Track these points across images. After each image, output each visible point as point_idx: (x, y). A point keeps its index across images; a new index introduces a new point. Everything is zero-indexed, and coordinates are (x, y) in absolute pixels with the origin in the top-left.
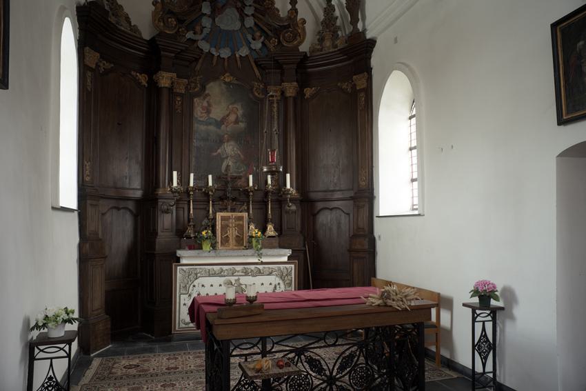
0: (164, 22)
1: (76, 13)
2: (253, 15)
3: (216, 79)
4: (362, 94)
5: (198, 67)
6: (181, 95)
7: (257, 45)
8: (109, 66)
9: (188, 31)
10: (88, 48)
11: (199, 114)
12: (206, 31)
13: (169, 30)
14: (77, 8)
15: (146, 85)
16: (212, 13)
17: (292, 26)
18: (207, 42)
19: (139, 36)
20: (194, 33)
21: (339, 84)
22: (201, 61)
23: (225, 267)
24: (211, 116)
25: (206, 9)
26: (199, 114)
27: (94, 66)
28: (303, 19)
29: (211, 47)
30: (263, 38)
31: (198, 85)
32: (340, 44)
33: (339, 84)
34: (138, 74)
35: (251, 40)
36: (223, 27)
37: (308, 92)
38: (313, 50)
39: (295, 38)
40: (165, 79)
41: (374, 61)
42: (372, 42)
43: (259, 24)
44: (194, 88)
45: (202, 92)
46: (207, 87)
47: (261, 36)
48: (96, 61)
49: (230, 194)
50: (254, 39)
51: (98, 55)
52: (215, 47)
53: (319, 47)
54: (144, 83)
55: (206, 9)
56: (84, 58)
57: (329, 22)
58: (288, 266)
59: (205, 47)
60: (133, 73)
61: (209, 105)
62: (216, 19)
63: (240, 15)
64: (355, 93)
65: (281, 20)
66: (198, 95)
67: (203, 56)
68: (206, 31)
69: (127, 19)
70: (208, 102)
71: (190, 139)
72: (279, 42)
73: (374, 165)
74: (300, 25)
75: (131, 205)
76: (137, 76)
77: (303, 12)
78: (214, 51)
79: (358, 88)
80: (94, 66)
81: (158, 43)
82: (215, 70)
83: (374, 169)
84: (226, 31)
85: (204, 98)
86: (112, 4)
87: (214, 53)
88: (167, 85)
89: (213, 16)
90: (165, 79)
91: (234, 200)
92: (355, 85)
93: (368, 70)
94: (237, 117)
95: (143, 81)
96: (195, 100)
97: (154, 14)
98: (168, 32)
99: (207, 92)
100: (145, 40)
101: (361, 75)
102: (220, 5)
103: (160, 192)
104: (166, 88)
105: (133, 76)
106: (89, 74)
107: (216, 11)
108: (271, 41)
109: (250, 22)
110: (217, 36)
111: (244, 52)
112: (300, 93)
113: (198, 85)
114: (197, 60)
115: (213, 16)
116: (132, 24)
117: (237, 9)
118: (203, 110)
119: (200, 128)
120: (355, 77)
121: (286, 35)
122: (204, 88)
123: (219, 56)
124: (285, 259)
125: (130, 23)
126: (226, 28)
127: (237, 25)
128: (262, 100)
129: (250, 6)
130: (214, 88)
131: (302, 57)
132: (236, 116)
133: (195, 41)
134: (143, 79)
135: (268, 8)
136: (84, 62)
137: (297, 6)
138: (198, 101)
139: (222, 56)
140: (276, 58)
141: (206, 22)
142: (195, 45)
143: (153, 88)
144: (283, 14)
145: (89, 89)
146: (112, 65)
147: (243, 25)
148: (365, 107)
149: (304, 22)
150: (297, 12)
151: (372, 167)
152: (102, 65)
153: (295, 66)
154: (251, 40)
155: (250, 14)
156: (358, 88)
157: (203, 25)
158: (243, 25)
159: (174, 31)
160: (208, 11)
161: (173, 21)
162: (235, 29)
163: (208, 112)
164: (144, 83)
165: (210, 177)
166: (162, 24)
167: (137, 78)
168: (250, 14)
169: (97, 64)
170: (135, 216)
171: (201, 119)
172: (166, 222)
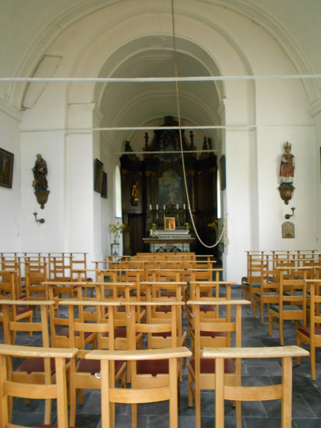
23: (167, 236)
37: (199, 173)
40: (148, 173)
45: (161, 176)
49: (171, 212)
58: (188, 235)
78: (165, 161)
90: (148, 173)
91: (173, 213)
103: (148, 211)
119: (161, 189)
124: (187, 233)
130: (166, 174)
134: (141, 174)
139: (168, 162)
143: (144, 175)
163: (163, 182)
164: (141, 175)
165: (164, 205)
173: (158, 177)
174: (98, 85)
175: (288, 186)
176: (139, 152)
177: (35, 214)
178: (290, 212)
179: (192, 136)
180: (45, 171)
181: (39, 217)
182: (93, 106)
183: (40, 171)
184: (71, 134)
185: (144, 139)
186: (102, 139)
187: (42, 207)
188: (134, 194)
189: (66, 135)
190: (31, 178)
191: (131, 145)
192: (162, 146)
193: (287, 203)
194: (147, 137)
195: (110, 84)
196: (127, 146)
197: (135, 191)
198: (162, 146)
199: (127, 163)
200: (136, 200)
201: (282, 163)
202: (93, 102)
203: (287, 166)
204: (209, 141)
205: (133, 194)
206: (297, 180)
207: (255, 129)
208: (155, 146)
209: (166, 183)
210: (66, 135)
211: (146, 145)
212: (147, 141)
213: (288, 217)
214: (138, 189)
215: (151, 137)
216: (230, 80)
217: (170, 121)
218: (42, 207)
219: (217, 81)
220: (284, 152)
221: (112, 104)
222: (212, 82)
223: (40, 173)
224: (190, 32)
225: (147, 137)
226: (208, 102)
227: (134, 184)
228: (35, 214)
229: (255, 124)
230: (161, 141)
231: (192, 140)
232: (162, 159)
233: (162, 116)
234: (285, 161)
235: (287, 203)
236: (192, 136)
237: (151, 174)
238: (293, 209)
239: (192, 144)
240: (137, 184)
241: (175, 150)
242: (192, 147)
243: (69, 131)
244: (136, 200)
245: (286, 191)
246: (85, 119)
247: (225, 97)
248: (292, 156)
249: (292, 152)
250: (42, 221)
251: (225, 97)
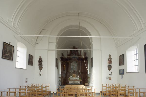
45: (72, 63)
49: (74, 72)
75: (65, 73)
90: (68, 62)
103: (68, 72)
119: (72, 66)
130: (73, 62)
134: (66, 62)
163: (72, 64)
170: (66, 74)
172: (68, 75)
174: (57, 37)
175: (110, 66)
176: (66, 56)
177: (39, 73)
178: (111, 73)
179: (80, 52)
180: (42, 61)
181: (40, 74)
182: (56, 43)
183: (40, 61)
184: (49, 51)
185: (67, 53)
186: (58, 53)
187: (41, 71)
189: (48, 51)
190: (38, 63)
191: (63, 54)
192: (72, 54)
193: (110, 71)
194: (68, 52)
195: (60, 37)
196: (63, 55)
198: (72, 54)
199: (62, 59)
200: (65, 69)
201: (109, 60)
202: (56, 42)
203: (110, 61)
204: (85, 53)
206: (112, 65)
207: (101, 51)
208: (70, 55)
209: (73, 65)
210: (48, 51)
211: (68, 54)
212: (68, 53)
213: (110, 75)
215: (69, 52)
216: (94, 37)
217: (74, 48)
218: (41, 71)
219: (90, 38)
220: (109, 57)
221: (61, 43)
222: (89, 38)
223: (40, 61)
224: (83, 25)
225: (68, 52)
226: (88, 43)
227: (64, 65)
228: (39, 73)
229: (101, 49)
230: (72, 53)
232: (72, 58)
233: (72, 46)
234: (109, 59)
235: (110, 71)
238: (112, 72)
239: (80, 54)
241: (76, 56)
242: (80, 55)
243: (49, 50)
244: (65, 69)
245: (110, 68)
246: (53, 47)
247: (93, 42)
248: (111, 58)
249: (111, 57)
250: (41, 75)
251: (93, 42)
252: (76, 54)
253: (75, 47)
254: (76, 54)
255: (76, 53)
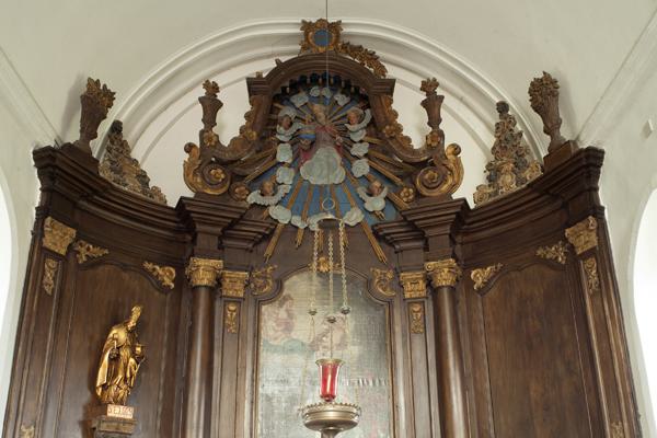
0: (203, 177)
1: (33, 163)
2: (366, 155)
3: (302, 267)
4: (592, 262)
5: (269, 251)
6: (238, 301)
7: (376, 204)
8: (97, 252)
9: (250, 192)
10: (49, 218)
11: (271, 333)
12: (282, 191)
13: (212, 189)
14: (35, 153)
15: (173, 285)
16: (294, 160)
17: (438, 160)
18: (286, 207)
19: (162, 203)
20: (262, 195)
21: (539, 252)
22: (274, 239)
24: (294, 335)
25: (284, 154)
26: (271, 333)
27: (63, 252)
28: (453, 145)
29: (292, 215)
30: (386, 189)
31: (270, 281)
32: (531, 175)
33: (539, 252)
34: (158, 268)
35: (363, 195)
36: (314, 180)
37: (479, 276)
38: (479, 196)
39: (444, 180)
40: (203, 271)
41: (606, 193)
42: (594, 158)
43: (379, 168)
44: (262, 287)
45: (277, 294)
46: (287, 283)
47: (382, 188)
48: (69, 242)
50: (371, 195)
51: (74, 232)
52: (301, 215)
53: (491, 190)
54: (168, 282)
55: (284, 154)
56: (43, 236)
57: (507, 139)
59: (282, 215)
60: (149, 266)
61: (290, 316)
62: (301, 169)
63: (344, 157)
64: (574, 258)
65: (414, 152)
66: (270, 299)
67: (278, 231)
68: (282, 191)
69: (143, 178)
70: (287, 311)
71: (255, 381)
72: (418, 195)
73: (640, 411)
74: (451, 157)
76: (154, 270)
77: (452, 133)
79: (579, 252)
80: (63, 252)
81: (188, 208)
82: (294, 253)
83: (641, 420)
84: (320, 187)
85: (281, 306)
86: (117, 157)
87: (299, 225)
88: (205, 282)
89: (296, 164)
90: (203, 271)
92: (572, 248)
93: (598, 212)
94: (344, 337)
95: (165, 279)
96: (264, 308)
97: (187, 167)
98: (209, 192)
99: (285, 293)
100: (172, 209)
101: (581, 225)
102: (305, 143)
104: (205, 286)
105: (146, 270)
106: (51, 263)
107: (303, 150)
108: (402, 194)
109: (362, 168)
110: (305, 196)
111: (354, 217)
112: (464, 280)
113: (270, 281)
114: (267, 238)
115: (296, 164)
116: (151, 185)
117: (338, 148)
118: (278, 325)
120: (568, 231)
121: (427, 176)
122: (280, 286)
123: (307, 228)
125: (146, 183)
126: (319, 183)
127: (339, 176)
128: (390, 303)
129: (361, 141)
130: (300, 286)
131: (458, 210)
132: (341, 333)
133: (265, 207)
134: (167, 275)
135: (392, 138)
136: (41, 242)
137: (441, 127)
138: (270, 309)
140: (409, 219)
141: (284, 177)
142: (265, 214)
144: (417, 143)
145: (50, 292)
146: (106, 252)
147: (349, 173)
148: (600, 286)
149: (456, 149)
150: (441, 135)
151: (637, 416)
152: (83, 250)
153: (447, 229)
154: (363, 195)
155: (361, 154)
156: (579, 252)
157: (279, 180)
158: (349, 173)
159: (224, 189)
160: (287, 157)
161: (219, 174)
162: (336, 182)
163: (288, 328)
164: (168, 282)
166: (199, 180)
167: (155, 274)
168: (361, 154)
169: (70, 247)
171: (275, 343)
173: (259, 303)
179: (432, 104)
185: (199, 111)
188: (112, 375)
194: (211, 105)
197: (115, 359)
205: (101, 378)
214: (139, 349)
225: (211, 105)
227: (118, 320)
230: (283, 134)
231: (434, 120)
236: (432, 104)
237: (219, 280)
240: (132, 324)
244: (115, 411)
252: (360, 150)
253: (336, 27)
254: (360, 150)
255: (358, 132)
